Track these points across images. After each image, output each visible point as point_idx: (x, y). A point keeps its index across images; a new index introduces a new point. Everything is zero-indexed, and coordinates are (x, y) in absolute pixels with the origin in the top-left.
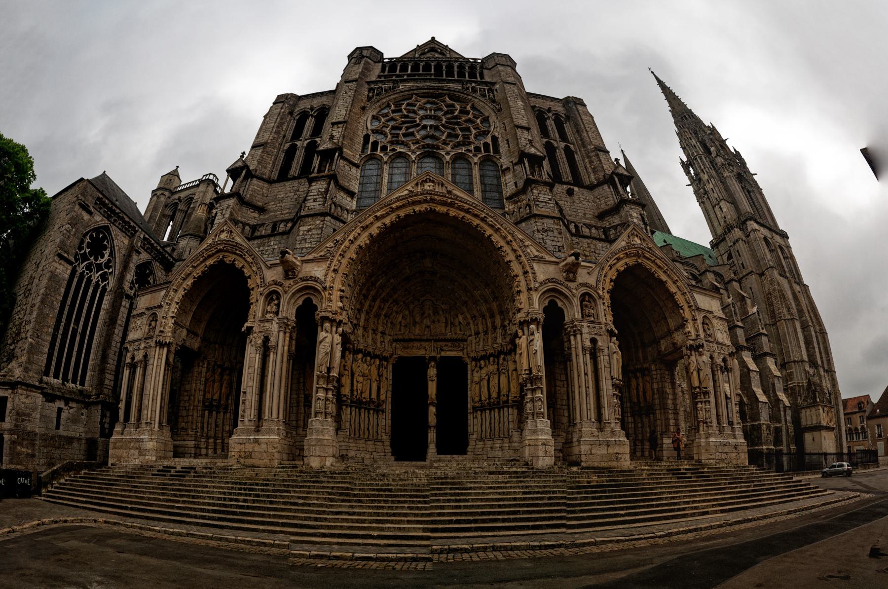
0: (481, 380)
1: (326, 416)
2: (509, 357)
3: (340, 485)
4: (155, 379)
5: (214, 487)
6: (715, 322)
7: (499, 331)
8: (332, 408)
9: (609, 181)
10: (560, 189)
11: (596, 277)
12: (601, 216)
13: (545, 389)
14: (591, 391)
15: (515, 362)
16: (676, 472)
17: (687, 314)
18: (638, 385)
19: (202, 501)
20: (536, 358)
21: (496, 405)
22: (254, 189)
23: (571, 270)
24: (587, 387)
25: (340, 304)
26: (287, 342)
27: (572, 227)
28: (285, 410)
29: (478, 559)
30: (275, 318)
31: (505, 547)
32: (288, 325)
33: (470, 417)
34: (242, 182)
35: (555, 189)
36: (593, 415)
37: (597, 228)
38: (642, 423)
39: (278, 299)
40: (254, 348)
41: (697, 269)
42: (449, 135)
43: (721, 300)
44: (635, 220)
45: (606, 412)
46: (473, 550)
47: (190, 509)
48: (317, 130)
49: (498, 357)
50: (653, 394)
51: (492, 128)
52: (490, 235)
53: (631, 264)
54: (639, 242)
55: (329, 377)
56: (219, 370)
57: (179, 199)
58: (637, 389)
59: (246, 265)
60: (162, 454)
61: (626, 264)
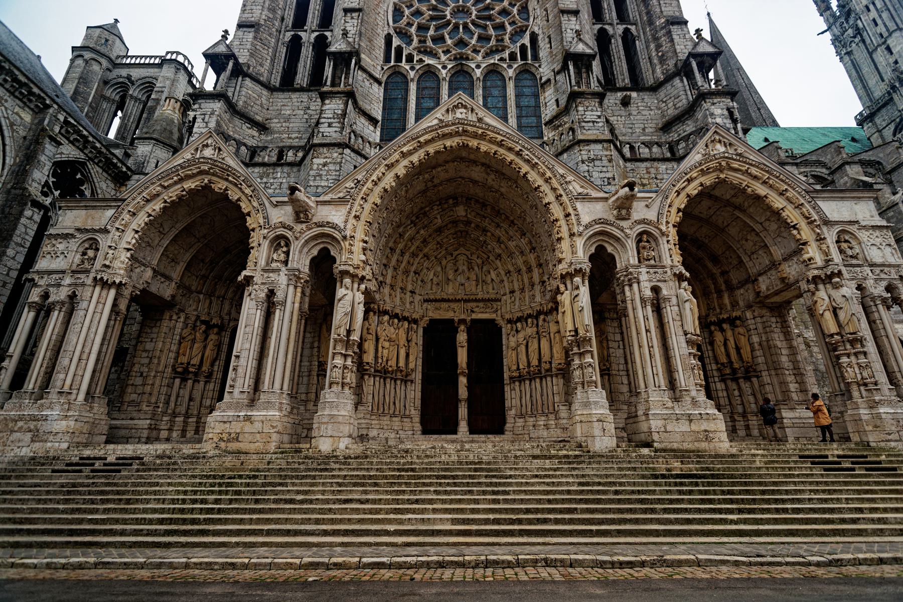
0: (518, 346)
1: (343, 387)
2: (549, 318)
3: (355, 473)
4: (91, 328)
5: (169, 484)
6: (863, 235)
7: (538, 288)
8: (351, 378)
9: (684, 70)
10: (613, 99)
11: (659, 208)
12: (667, 127)
13: (595, 353)
14: (657, 351)
15: (557, 322)
16: (819, 460)
17: (806, 233)
18: (726, 340)
19: (141, 506)
20: (583, 316)
21: (538, 374)
22: (247, 93)
23: (624, 207)
24: (650, 347)
25: (363, 258)
26: (298, 299)
27: (626, 151)
28: (292, 379)
29: (525, 578)
30: (284, 269)
31: (562, 561)
32: (299, 278)
33: (507, 389)
34: (229, 79)
35: (606, 101)
36: (662, 381)
37: (659, 145)
38: (740, 389)
39: (288, 245)
40: (254, 302)
41: (824, 165)
42: (480, 38)
43: (876, 200)
44: (719, 120)
45: (683, 378)
46: (519, 564)
47: (117, 521)
48: (326, 20)
49: (537, 318)
50: (753, 350)
51: (531, 19)
52: (526, 173)
53: (708, 183)
54: (722, 149)
55: (348, 341)
56: (203, 327)
57: (129, 77)
58: (725, 345)
59: (243, 197)
60: (83, 439)
61: (702, 185)
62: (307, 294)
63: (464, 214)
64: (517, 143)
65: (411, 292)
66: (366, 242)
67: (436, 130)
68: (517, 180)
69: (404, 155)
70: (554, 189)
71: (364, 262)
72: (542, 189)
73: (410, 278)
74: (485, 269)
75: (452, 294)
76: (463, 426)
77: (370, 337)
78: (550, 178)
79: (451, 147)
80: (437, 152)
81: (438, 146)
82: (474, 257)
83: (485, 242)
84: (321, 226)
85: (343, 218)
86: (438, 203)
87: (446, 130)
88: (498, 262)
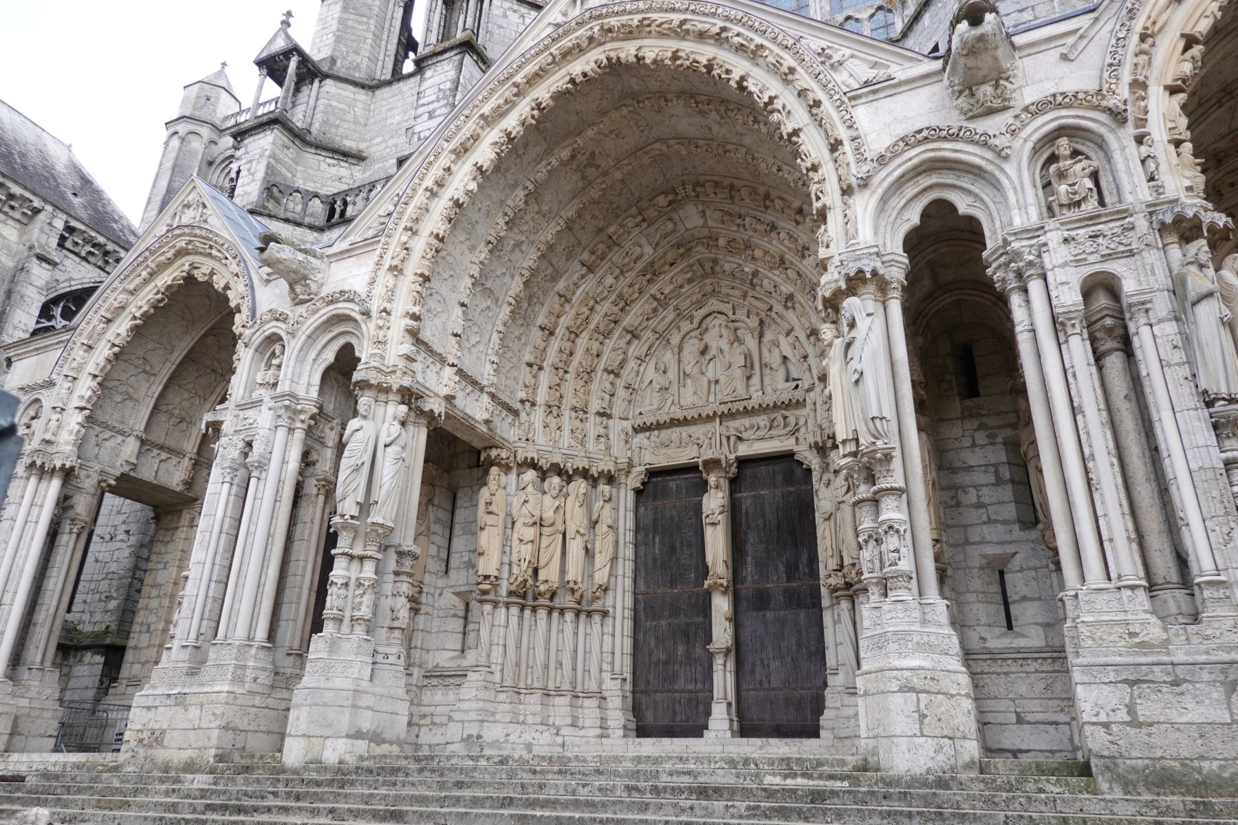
62: (330, 444)
63: (700, 222)
64: (714, 15)
65: (601, 414)
66: (415, 317)
67: (547, 47)
68: (739, 104)
69: (488, 121)
70: (802, 93)
71: (409, 359)
72: (778, 104)
73: (594, 386)
74: (768, 336)
75: (695, 406)
76: (720, 719)
77: (490, 520)
78: (792, 70)
79: (585, 75)
80: (559, 96)
81: (558, 81)
82: (742, 314)
83: (755, 274)
84: (332, 302)
85: (367, 278)
86: (634, 210)
87: (567, 42)
88: (791, 315)
